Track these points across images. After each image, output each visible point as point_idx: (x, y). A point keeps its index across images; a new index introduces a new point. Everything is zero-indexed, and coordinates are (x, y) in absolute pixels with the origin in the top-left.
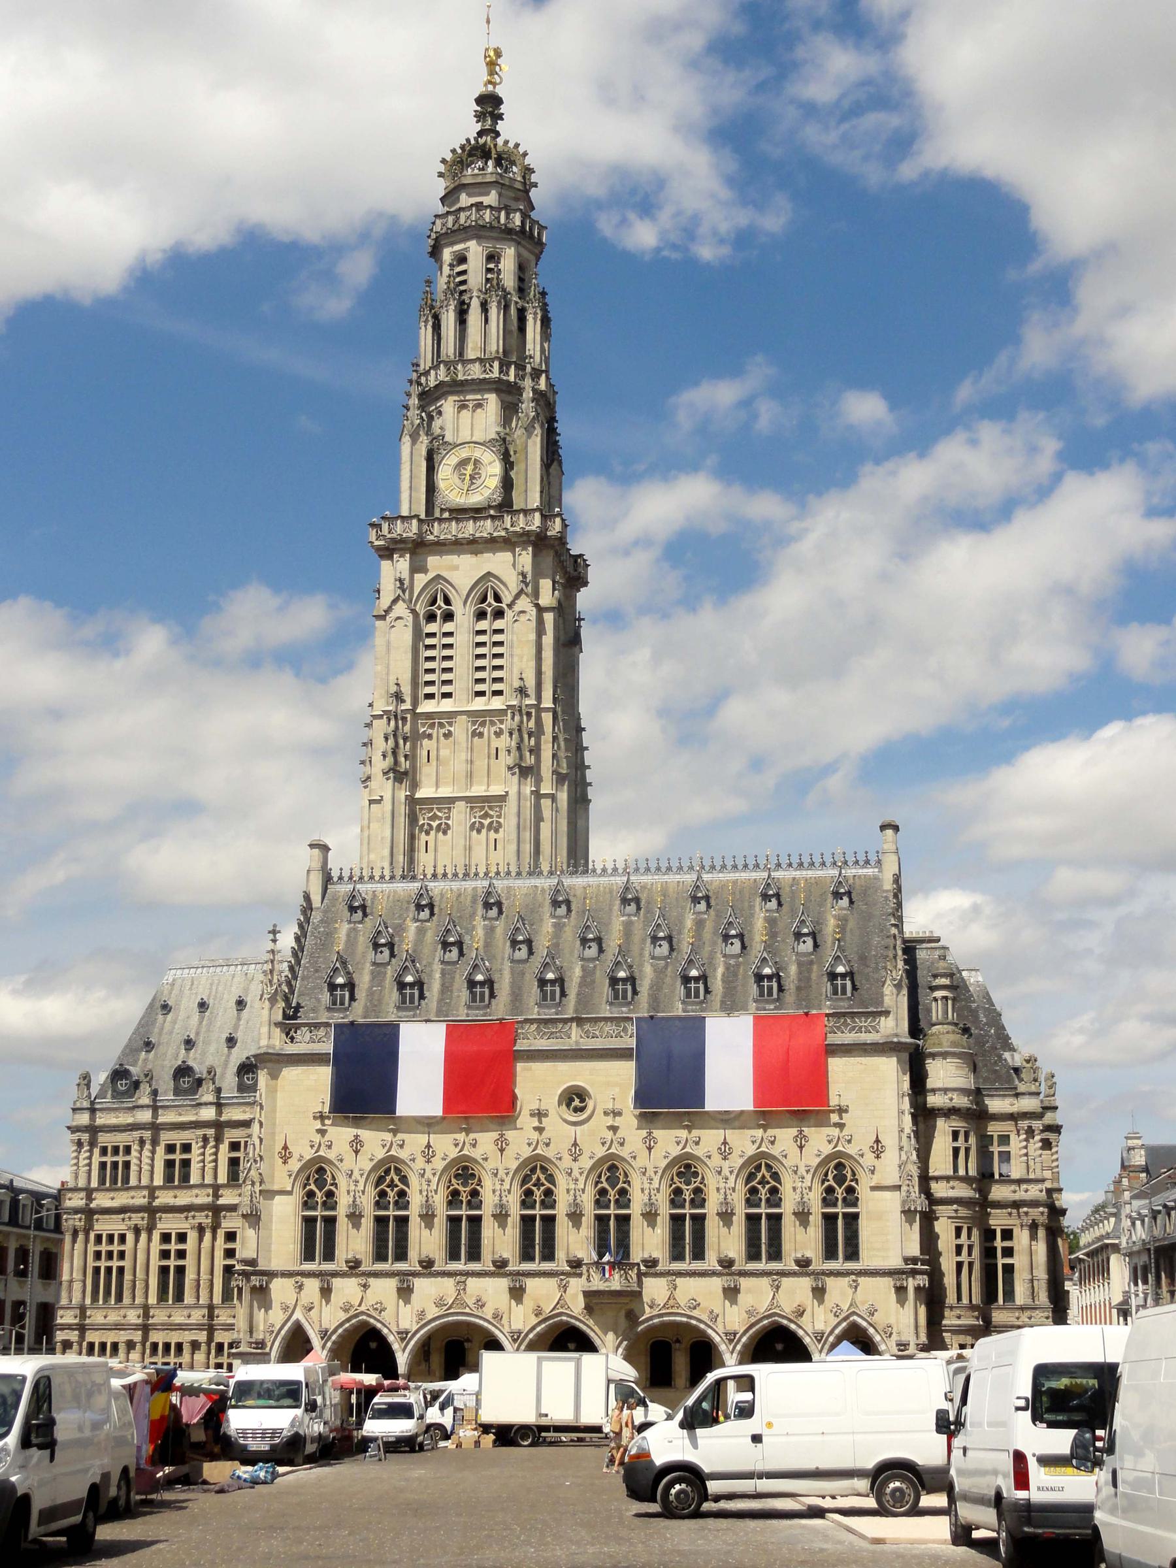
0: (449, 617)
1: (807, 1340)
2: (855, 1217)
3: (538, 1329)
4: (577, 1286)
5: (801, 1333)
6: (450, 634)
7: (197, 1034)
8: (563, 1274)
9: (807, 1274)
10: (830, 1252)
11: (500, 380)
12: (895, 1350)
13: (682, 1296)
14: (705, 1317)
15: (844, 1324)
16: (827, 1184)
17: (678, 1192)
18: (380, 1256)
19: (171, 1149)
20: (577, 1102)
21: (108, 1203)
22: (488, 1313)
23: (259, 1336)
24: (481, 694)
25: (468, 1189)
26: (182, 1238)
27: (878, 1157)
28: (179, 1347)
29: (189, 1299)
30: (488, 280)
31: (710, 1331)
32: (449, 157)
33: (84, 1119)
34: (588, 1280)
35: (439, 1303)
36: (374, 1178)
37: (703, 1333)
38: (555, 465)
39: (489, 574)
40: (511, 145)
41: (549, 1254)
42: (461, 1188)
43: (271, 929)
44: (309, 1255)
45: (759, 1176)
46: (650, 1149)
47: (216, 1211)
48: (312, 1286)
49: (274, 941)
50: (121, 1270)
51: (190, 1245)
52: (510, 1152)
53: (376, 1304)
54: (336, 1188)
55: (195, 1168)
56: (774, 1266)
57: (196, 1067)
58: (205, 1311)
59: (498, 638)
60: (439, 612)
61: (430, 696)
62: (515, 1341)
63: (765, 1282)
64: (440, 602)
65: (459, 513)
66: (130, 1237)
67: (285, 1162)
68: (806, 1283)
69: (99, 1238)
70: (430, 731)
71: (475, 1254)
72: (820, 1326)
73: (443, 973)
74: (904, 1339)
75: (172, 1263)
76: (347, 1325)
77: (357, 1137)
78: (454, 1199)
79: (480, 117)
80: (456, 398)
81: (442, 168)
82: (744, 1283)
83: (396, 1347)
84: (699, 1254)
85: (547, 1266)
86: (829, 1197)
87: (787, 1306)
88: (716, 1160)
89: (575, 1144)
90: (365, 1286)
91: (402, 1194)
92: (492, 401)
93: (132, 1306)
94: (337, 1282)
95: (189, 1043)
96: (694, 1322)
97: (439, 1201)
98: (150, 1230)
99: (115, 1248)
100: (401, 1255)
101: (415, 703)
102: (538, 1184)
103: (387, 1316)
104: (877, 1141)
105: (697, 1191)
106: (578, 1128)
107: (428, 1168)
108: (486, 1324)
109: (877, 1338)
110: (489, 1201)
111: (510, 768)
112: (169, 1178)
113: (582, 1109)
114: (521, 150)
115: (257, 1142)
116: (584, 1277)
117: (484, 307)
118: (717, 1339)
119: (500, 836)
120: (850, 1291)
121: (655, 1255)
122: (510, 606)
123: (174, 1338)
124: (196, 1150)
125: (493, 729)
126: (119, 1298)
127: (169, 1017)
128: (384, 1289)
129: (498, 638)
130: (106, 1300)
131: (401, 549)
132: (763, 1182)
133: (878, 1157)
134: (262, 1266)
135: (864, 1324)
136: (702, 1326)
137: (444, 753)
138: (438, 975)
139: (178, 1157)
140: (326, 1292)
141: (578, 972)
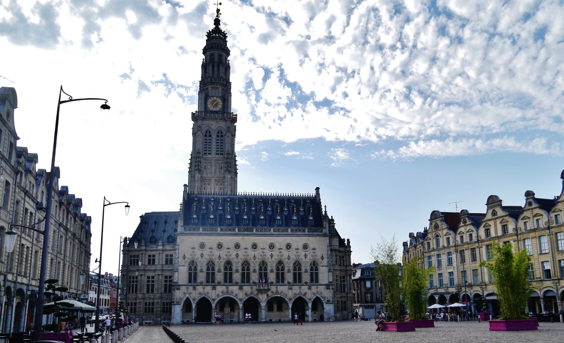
0: (210, 136)
1: (307, 300)
3: (246, 298)
4: (255, 288)
5: (306, 298)
6: (211, 140)
7: (155, 229)
9: (307, 285)
11: (222, 83)
12: (326, 302)
13: (279, 291)
14: (284, 295)
15: (315, 297)
18: (208, 281)
19: (149, 256)
20: (254, 247)
21: (132, 269)
22: (234, 294)
23: (177, 301)
24: (218, 154)
26: (153, 277)
27: (322, 260)
28: (153, 303)
29: (155, 292)
30: (219, 60)
31: (286, 299)
32: (208, 32)
33: (127, 248)
35: (223, 292)
36: (206, 263)
37: (284, 299)
39: (220, 126)
41: (248, 281)
44: (190, 281)
45: (296, 264)
46: (272, 257)
47: (163, 270)
48: (191, 288)
50: (136, 285)
51: (155, 279)
52: (239, 257)
56: (300, 284)
57: (156, 237)
58: (160, 295)
59: (222, 142)
60: (208, 135)
61: (206, 154)
62: (240, 300)
63: (297, 287)
66: (139, 277)
67: (184, 259)
68: (306, 287)
70: (206, 162)
71: (231, 281)
72: (310, 297)
73: (219, 216)
74: (329, 299)
75: (150, 283)
76: (200, 298)
77: (202, 253)
78: (226, 268)
79: (215, 24)
80: (212, 86)
82: (294, 287)
83: (212, 303)
84: (283, 281)
85: (248, 284)
86: (312, 269)
87: (303, 293)
88: (287, 260)
89: (254, 256)
90: (204, 288)
91: (213, 267)
93: (140, 293)
94: (198, 287)
95: (153, 231)
96: (282, 296)
97: (222, 268)
98: (144, 275)
99: (135, 280)
100: (213, 281)
101: (203, 155)
102: (246, 265)
103: (209, 295)
104: (322, 256)
106: (255, 252)
107: (219, 261)
108: (234, 297)
109: (323, 300)
110: (234, 268)
111: (225, 171)
112: (149, 263)
113: (255, 248)
115: (178, 254)
116: (258, 286)
119: (222, 186)
120: (316, 289)
121: (273, 281)
122: (225, 134)
123: (151, 301)
125: (221, 162)
126: (136, 292)
127: (146, 225)
128: (208, 289)
129: (222, 142)
130: (133, 293)
133: (322, 260)
134: (179, 283)
135: (319, 296)
137: (209, 167)
138: (218, 217)
139: (152, 258)
140: (195, 289)
141: (251, 217)
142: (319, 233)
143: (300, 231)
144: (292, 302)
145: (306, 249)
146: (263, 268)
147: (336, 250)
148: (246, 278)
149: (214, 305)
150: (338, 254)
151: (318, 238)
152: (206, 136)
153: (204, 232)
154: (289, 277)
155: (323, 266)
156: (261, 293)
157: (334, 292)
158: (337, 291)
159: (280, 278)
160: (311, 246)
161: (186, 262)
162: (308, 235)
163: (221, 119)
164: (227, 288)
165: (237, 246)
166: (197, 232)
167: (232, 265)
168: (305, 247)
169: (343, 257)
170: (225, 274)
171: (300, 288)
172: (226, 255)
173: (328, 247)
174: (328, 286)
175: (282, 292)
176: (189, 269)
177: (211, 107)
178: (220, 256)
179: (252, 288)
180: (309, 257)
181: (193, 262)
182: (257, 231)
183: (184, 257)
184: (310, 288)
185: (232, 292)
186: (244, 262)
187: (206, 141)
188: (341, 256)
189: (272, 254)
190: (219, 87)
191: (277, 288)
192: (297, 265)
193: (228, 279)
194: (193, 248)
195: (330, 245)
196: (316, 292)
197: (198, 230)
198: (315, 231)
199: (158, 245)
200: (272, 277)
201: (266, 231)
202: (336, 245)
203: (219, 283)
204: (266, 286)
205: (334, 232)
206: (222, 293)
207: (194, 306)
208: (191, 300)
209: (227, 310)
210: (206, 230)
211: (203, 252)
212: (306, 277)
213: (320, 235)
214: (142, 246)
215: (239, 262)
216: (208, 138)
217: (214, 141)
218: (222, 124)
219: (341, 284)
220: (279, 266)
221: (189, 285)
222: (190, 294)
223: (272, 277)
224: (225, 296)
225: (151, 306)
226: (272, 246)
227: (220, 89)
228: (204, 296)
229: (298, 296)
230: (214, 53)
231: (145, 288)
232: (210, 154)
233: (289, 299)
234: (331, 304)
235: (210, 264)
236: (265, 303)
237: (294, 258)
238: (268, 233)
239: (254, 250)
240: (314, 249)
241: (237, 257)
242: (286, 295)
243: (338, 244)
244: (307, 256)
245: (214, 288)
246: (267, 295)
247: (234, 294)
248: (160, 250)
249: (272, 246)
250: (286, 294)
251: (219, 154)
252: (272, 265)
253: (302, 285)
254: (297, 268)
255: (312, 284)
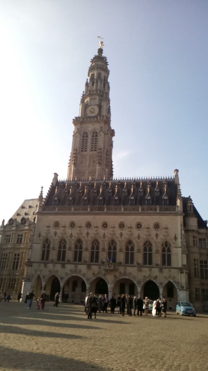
0: (87, 136)
1: (158, 285)
2: (170, 254)
3: (94, 278)
5: (156, 283)
8: (100, 265)
10: (164, 263)
11: (99, 94)
13: (127, 272)
16: (163, 247)
17: (127, 247)
18: (59, 259)
19: (19, 235)
20: (105, 225)
22: (82, 273)
24: (92, 151)
25: (80, 244)
26: (19, 255)
27: (176, 240)
34: (106, 267)
35: (71, 271)
38: (109, 114)
40: (104, 57)
41: (97, 261)
42: (78, 244)
43: (41, 187)
44: (43, 259)
45: (147, 244)
46: (121, 236)
48: (42, 265)
49: (42, 189)
52: (89, 236)
53: (57, 270)
54: (50, 244)
55: (23, 239)
56: (150, 266)
60: (85, 136)
61: (82, 151)
64: (85, 133)
65: (90, 117)
67: (39, 237)
69: (2, 254)
71: (80, 260)
75: (16, 261)
76: (50, 276)
77: (56, 232)
78: (76, 247)
81: (91, 61)
83: (60, 281)
84: (132, 262)
85: (96, 263)
88: (137, 239)
89: (104, 235)
90: (54, 266)
92: (97, 97)
96: (130, 278)
100: (63, 259)
102: (95, 244)
104: (175, 236)
105: (132, 247)
107: (71, 239)
109: (175, 285)
110: (84, 246)
113: (106, 227)
114: (106, 57)
116: (105, 266)
117: (97, 82)
118: (136, 283)
122: (98, 133)
124: (24, 236)
128: (58, 267)
131: (78, 123)
132: (148, 245)
133: (176, 240)
135: (172, 281)
136: (132, 280)
140: (46, 266)
142: (172, 212)
143: (151, 209)
144: (141, 286)
145: (158, 228)
146: (112, 247)
147: (193, 231)
148: (95, 257)
149: (62, 284)
150: (197, 235)
151: (170, 217)
152: (84, 137)
153: (59, 212)
154: (139, 258)
155: (176, 247)
156: (109, 273)
157: (189, 278)
158: (195, 277)
159: (129, 259)
160: (163, 224)
161: (40, 240)
162: (159, 213)
163: (96, 122)
164: (76, 267)
165: (89, 225)
166: (54, 212)
167: (82, 243)
168: (157, 226)
169: (204, 240)
170: (76, 252)
171: (150, 270)
172: (77, 233)
173: (181, 226)
174: (181, 270)
175: (130, 273)
176: (43, 247)
177: (89, 114)
178: (71, 234)
179: (100, 268)
180: (161, 237)
181: (47, 240)
182: (108, 210)
183: (40, 235)
184: (161, 271)
185: (80, 271)
186: (94, 240)
187: (83, 141)
188: (202, 238)
189: (121, 233)
190: (96, 98)
191: (125, 269)
192: (147, 245)
193: (78, 258)
194: (48, 227)
195: (185, 224)
196: (168, 276)
197: (54, 210)
198: (168, 210)
199: (25, 226)
200: (121, 257)
201: (117, 210)
202: (194, 226)
203: (69, 262)
204: (112, 266)
205: (192, 212)
206: (70, 271)
207: (44, 284)
208: (41, 277)
209: (79, 289)
210: (61, 209)
211: (56, 230)
212: (157, 259)
213: (172, 213)
214: (14, 226)
215: (89, 240)
216: (85, 138)
217: (89, 140)
218: (97, 126)
219: (202, 270)
220: (129, 246)
221: (40, 263)
222: (41, 271)
223: (121, 257)
224: (73, 275)
225: (13, 283)
226: (122, 226)
227: (98, 99)
228: (53, 274)
229: (148, 279)
230: (95, 73)
231: (12, 264)
232: (86, 151)
233: (138, 282)
234: (184, 292)
235: (62, 242)
236: (113, 285)
237: (145, 237)
238: (119, 212)
239: (104, 229)
240: (167, 228)
241: (88, 235)
242: (135, 277)
243: (197, 225)
244: (158, 235)
245: (63, 266)
246: (115, 276)
247: (82, 273)
248: (26, 230)
249: (122, 225)
250: (135, 276)
251: (94, 150)
252: (120, 245)
253: (153, 267)
254: (148, 248)
255: (164, 266)
